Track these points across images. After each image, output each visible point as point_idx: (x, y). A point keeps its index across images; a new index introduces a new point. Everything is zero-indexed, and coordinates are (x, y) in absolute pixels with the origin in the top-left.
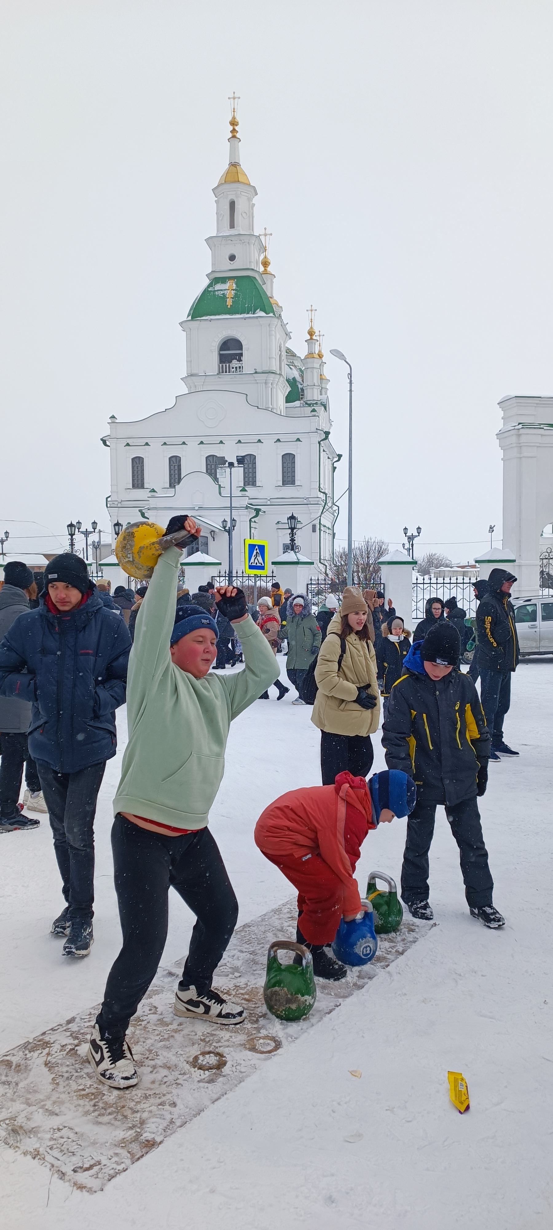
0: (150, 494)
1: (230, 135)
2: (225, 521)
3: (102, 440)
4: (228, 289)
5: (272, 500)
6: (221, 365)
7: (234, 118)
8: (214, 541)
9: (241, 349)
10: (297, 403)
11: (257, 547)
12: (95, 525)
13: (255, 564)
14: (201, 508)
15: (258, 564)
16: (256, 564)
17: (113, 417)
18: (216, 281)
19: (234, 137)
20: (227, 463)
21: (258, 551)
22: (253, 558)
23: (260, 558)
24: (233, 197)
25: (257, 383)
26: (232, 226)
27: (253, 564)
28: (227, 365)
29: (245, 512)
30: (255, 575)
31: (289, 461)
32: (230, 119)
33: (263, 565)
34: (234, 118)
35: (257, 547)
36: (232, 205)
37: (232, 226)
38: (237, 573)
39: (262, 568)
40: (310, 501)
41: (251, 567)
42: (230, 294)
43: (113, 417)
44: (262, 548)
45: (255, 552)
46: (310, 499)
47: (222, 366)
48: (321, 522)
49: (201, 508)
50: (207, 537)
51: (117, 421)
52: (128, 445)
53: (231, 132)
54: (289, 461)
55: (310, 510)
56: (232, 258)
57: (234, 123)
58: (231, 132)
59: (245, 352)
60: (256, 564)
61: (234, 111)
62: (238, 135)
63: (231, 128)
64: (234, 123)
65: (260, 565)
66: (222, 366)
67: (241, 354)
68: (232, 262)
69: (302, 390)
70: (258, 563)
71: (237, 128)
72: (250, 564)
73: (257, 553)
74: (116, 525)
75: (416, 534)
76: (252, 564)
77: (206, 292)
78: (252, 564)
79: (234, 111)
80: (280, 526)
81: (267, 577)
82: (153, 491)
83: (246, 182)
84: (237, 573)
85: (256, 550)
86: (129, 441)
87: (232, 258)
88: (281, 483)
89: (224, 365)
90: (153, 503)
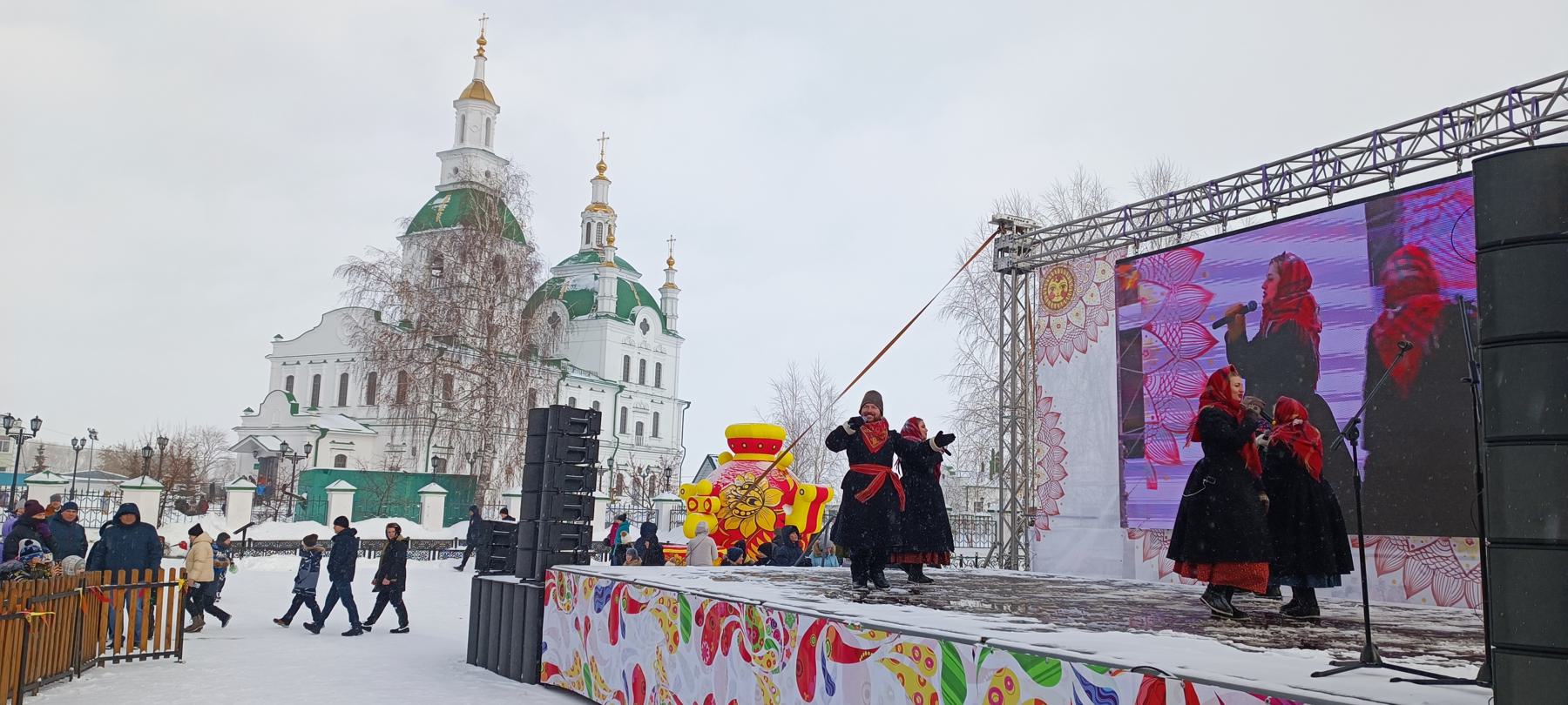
1: (476, 53)
2: (309, 445)
4: (442, 203)
7: (482, 37)
10: (586, 317)
12: (309, 448)
14: (277, 428)
17: (279, 336)
18: (442, 195)
19: (481, 55)
26: (462, 140)
29: (306, 432)
34: (482, 37)
36: (464, 118)
37: (462, 140)
42: (442, 207)
49: (277, 428)
52: (284, 364)
53: (478, 50)
56: (456, 171)
57: (482, 42)
58: (478, 50)
61: (482, 32)
62: (485, 54)
63: (478, 46)
64: (482, 42)
69: (597, 301)
71: (484, 47)
74: (73, 440)
77: (426, 205)
79: (482, 32)
86: (285, 360)
88: (336, 404)
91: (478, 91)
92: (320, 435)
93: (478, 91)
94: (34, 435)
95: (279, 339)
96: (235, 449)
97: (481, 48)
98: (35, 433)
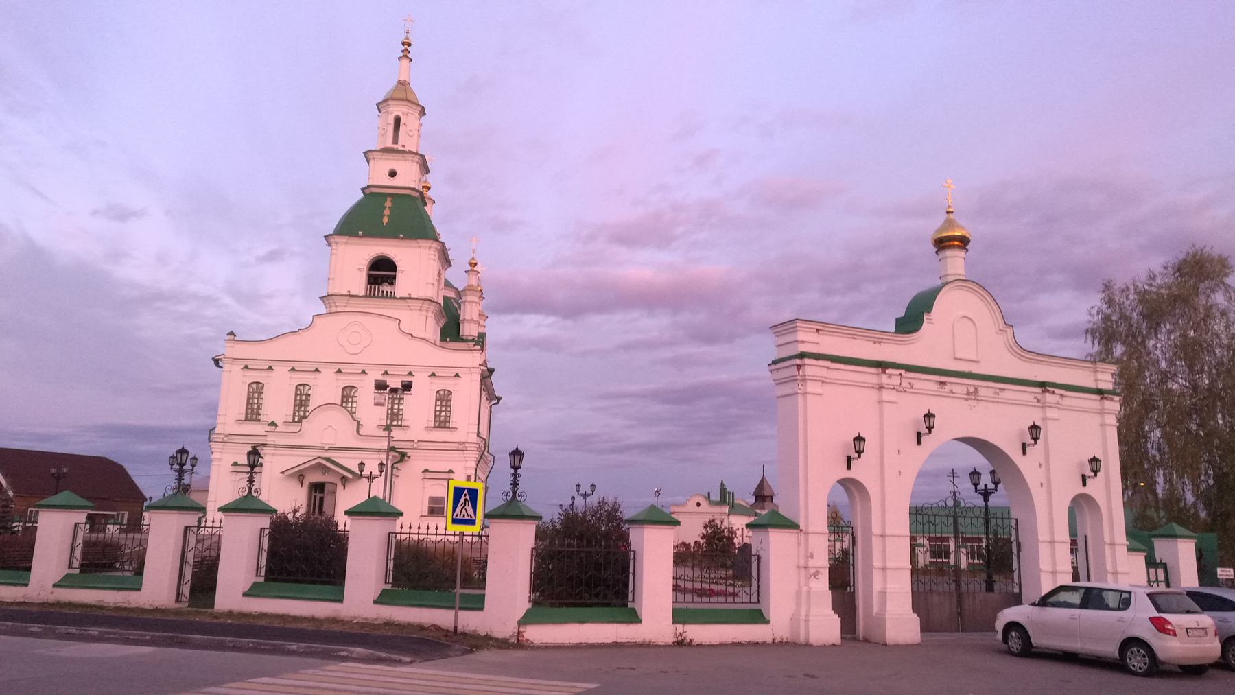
0: (268, 428)
1: (402, 54)
3: (213, 359)
5: (420, 443)
6: (369, 286)
7: (407, 38)
8: (344, 488)
9: (396, 271)
11: (466, 492)
13: (461, 517)
15: (466, 517)
16: (464, 516)
17: (231, 333)
19: (405, 56)
20: (388, 389)
21: (467, 497)
22: (459, 508)
23: (469, 508)
24: (400, 114)
25: (410, 309)
27: (458, 517)
28: (377, 287)
30: (460, 532)
31: (444, 399)
32: (402, 39)
33: (474, 518)
35: (466, 492)
38: (402, 527)
39: (473, 522)
40: (466, 447)
41: (455, 521)
43: (231, 333)
44: (473, 493)
45: (463, 498)
46: (467, 445)
47: (371, 288)
48: (477, 474)
50: (336, 485)
51: (236, 339)
53: (402, 51)
54: (444, 399)
55: (465, 457)
56: (393, 174)
59: (398, 275)
60: (464, 516)
62: (409, 55)
63: (403, 48)
65: (469, 518)
66: (371, 288)
67: (394, 277)
68: (392, 179)
70: (466, 515)
71: (409, 49)
72: (454, 517)
73: (466, 500)
75: (589, 492)
76: (457, 516)
78: (457, 516)
80: (428, 475)
81: (473, 535)
82: (273, 424)
83: (415, 101)
84: (402, 527)
85: (465, 495)
87: (393, 174)
89: (373, 287)
90: (271, 439)
91: (402, 92)
92: (399, 459)
93: (402, 92)
94: (996, 490)
95: (232, 337)
96: (286, 473)
97: (406, 50)
98: (996, 487)
